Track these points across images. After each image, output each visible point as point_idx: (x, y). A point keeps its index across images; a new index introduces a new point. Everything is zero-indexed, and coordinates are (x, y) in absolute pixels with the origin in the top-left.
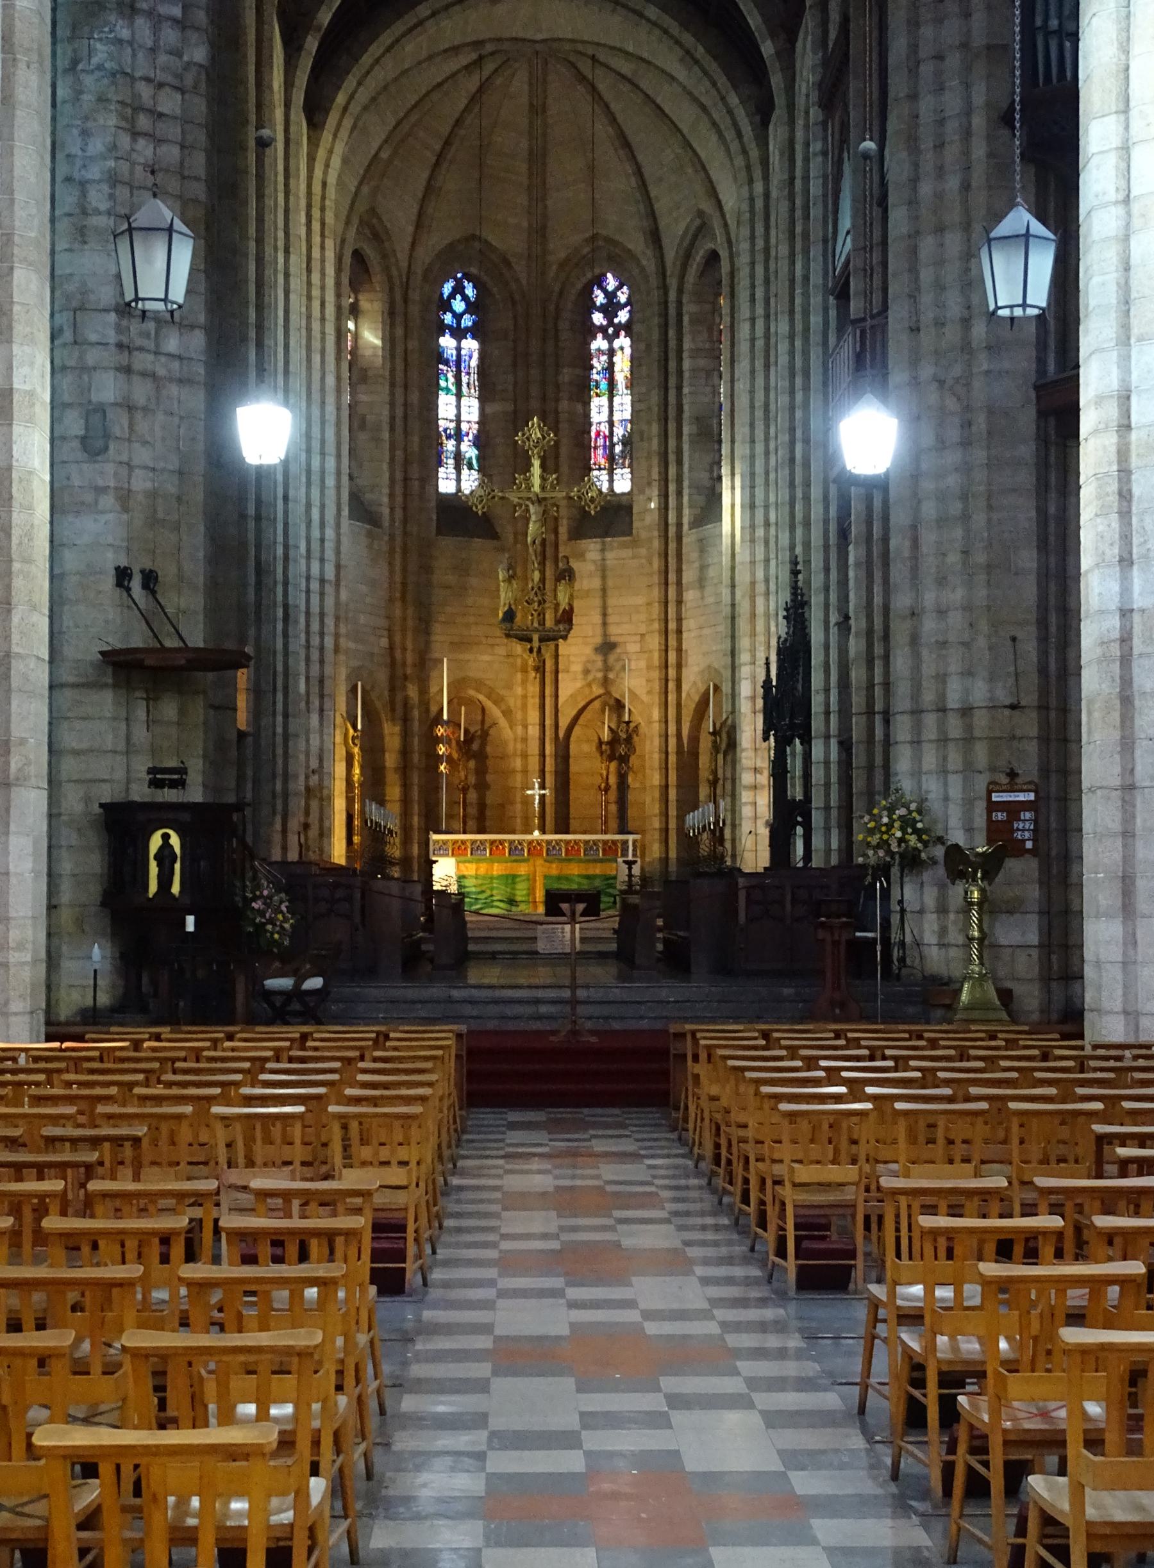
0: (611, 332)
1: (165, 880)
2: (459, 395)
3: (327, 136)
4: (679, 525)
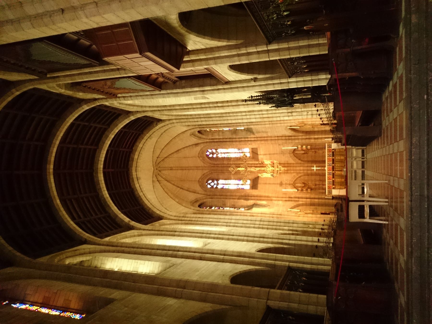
0: (217, 153)
4: (254, 138)
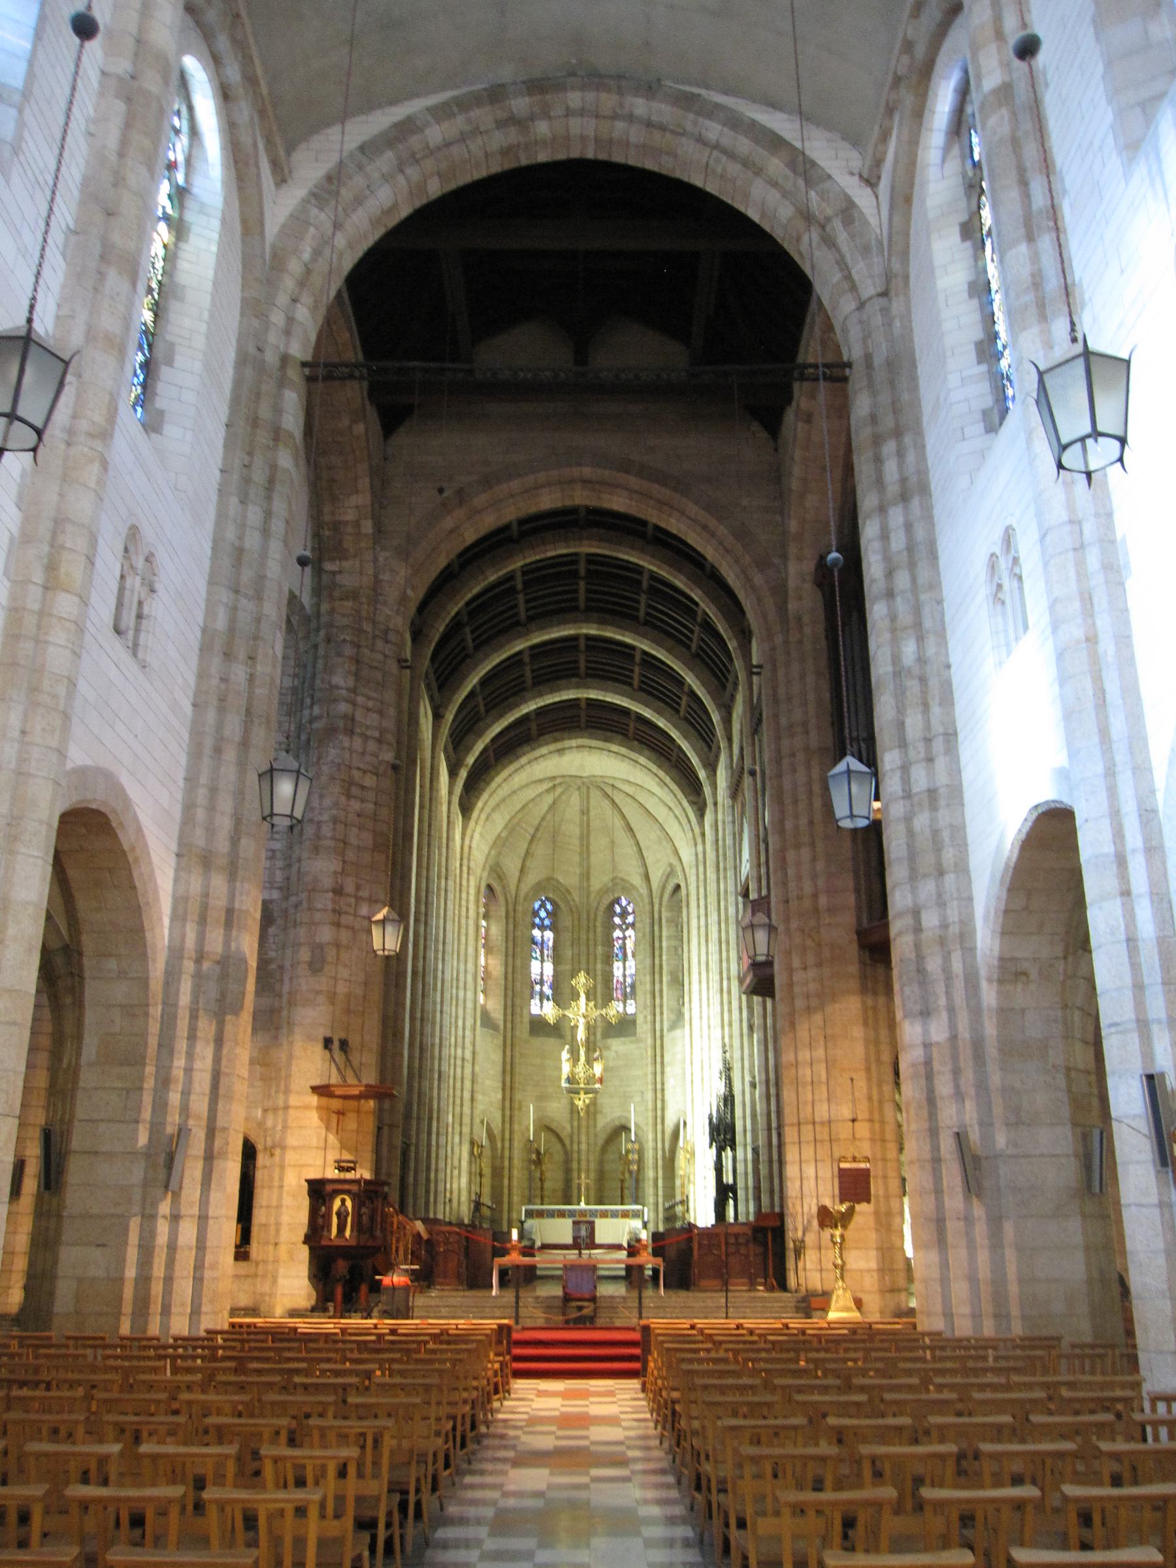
2: (542, 961)
3: (472, 823)
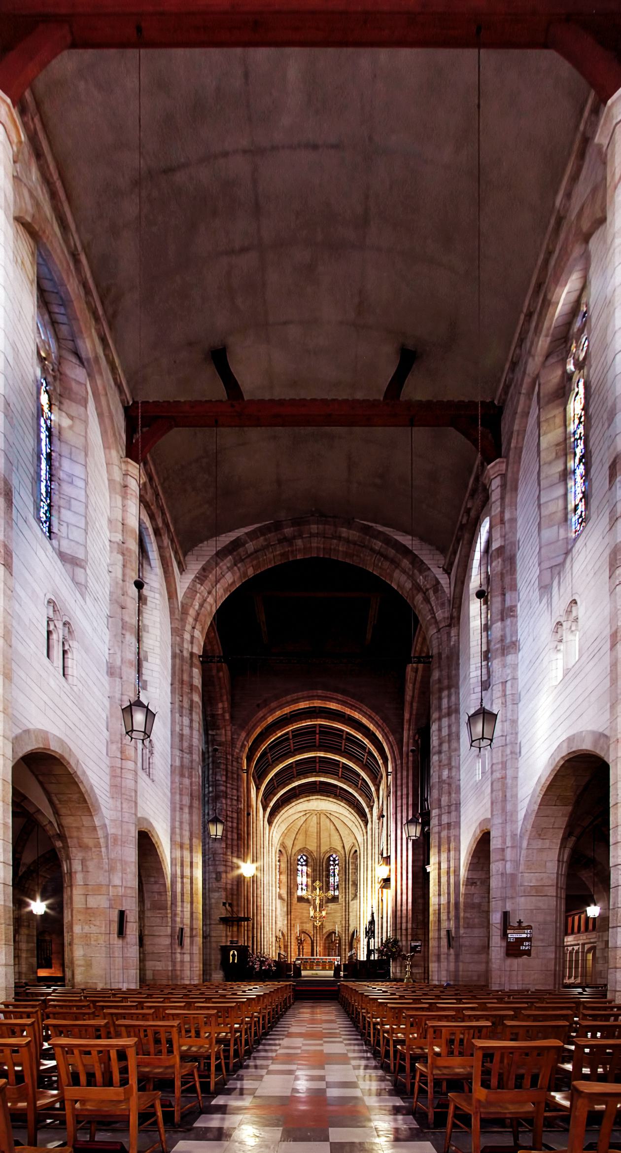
1: (234, 959)
3: (273, 828)
